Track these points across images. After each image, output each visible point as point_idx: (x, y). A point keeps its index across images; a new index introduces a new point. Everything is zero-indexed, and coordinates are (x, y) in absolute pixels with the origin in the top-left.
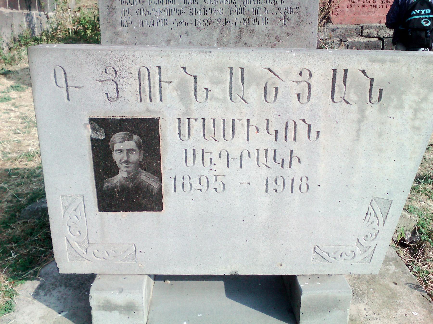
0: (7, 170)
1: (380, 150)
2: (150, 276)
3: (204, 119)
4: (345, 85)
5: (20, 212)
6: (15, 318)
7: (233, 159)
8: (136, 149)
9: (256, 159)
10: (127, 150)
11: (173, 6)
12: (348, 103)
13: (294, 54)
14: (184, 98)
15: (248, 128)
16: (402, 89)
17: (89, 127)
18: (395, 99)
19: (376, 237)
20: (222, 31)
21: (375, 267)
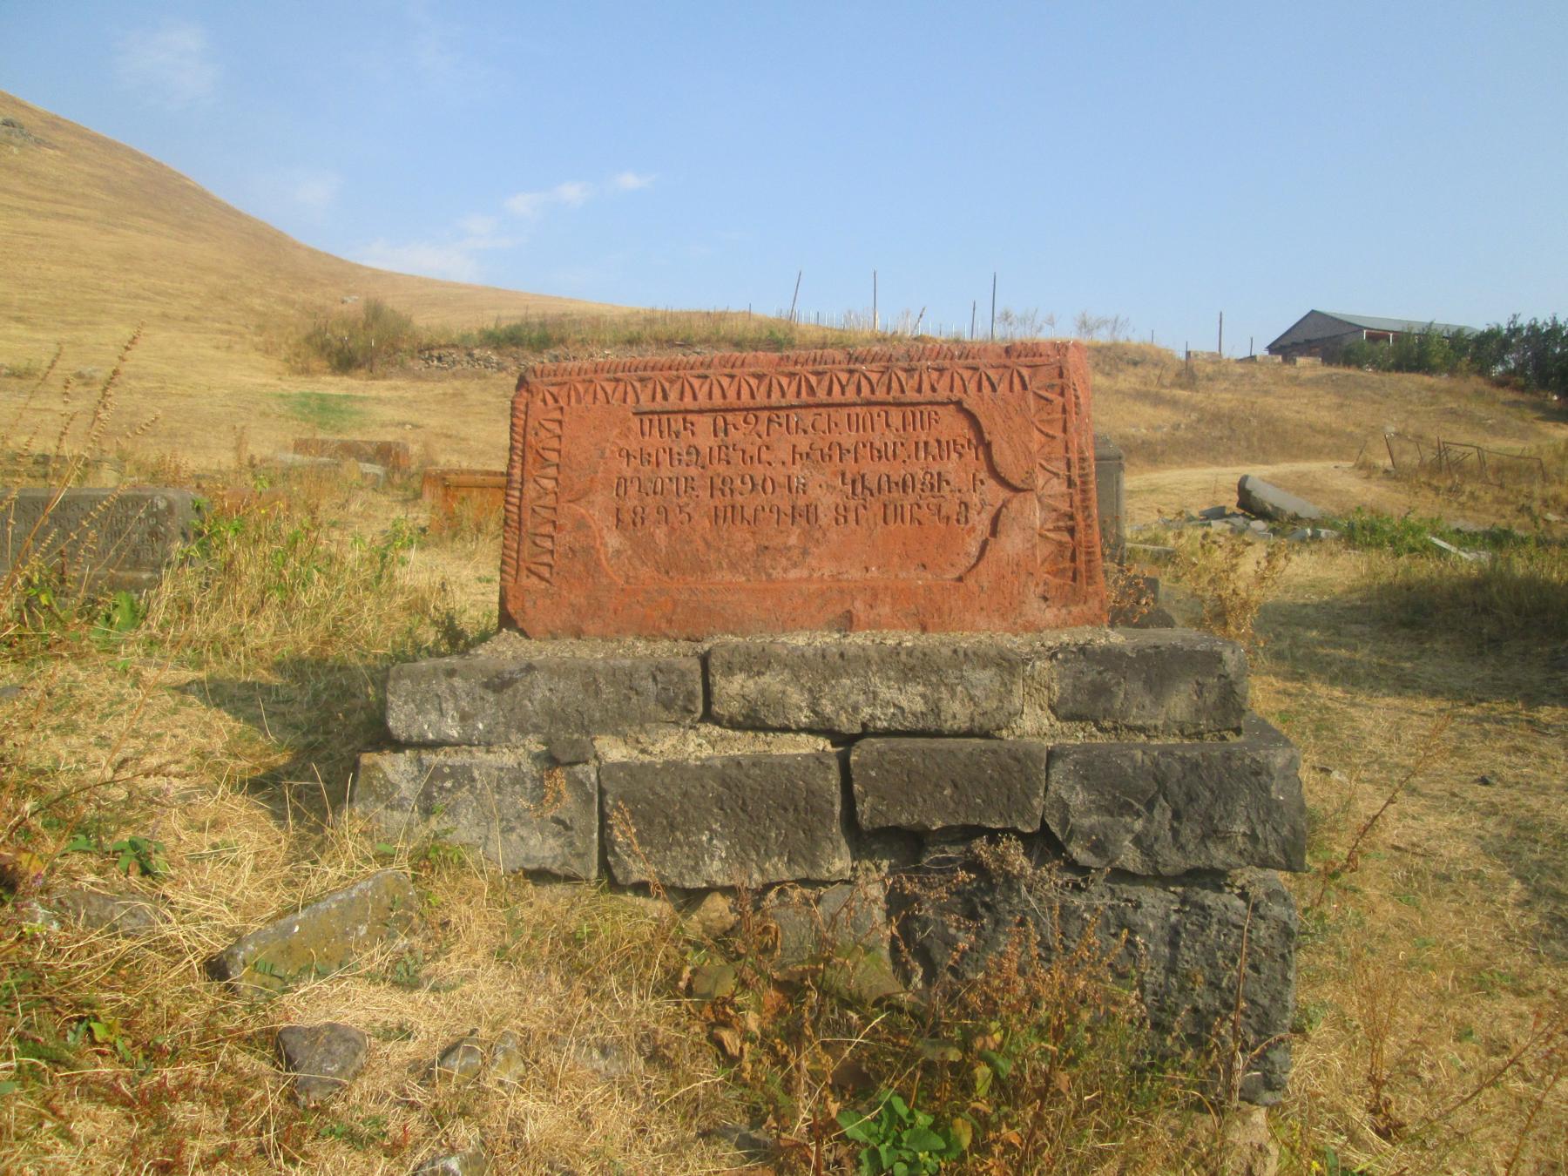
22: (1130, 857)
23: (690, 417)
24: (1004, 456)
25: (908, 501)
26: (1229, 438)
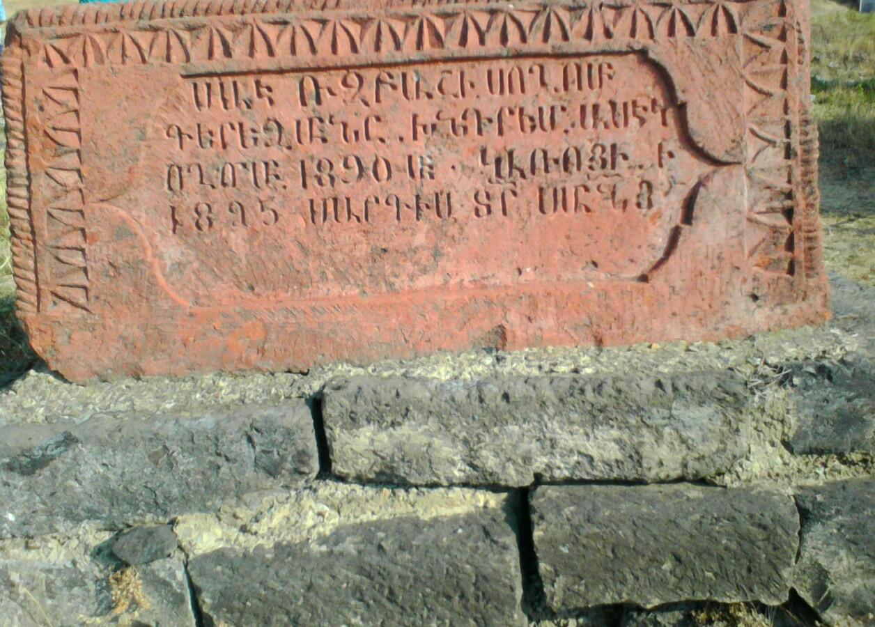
23: (265, 80)
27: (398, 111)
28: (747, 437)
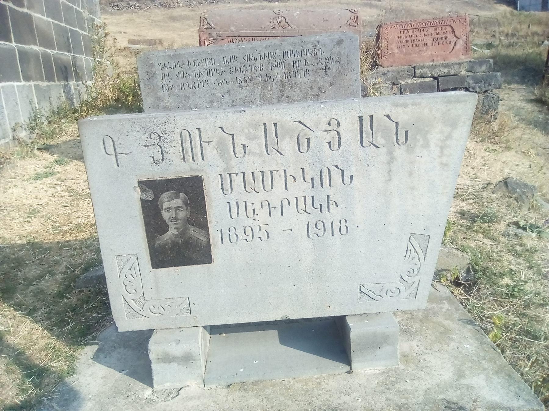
0: (58, 243)
1: (413, 188)
2: (205, 327)
3: (244, 173)
4: (372, 130)
5: (75, 282)
6: (78, 379)
7: (275, 208)
8: (184, 206)
9: (295, 207)
10: (175, 207)
11: (213, 66)
12: (376, 147)
13: (322, 106)
14: (223, 155)
15: (286, 178)
16: (426, 129)
17: (138, 189)
18: (421, 139)
19: (418, 272)
20: (264, 87)
21: (421, 303)
22: (478, 89)
24: (457, 33)
25: (442, 41)
26: (396, 18)
27: (423, 33)
28: (461, 69)
